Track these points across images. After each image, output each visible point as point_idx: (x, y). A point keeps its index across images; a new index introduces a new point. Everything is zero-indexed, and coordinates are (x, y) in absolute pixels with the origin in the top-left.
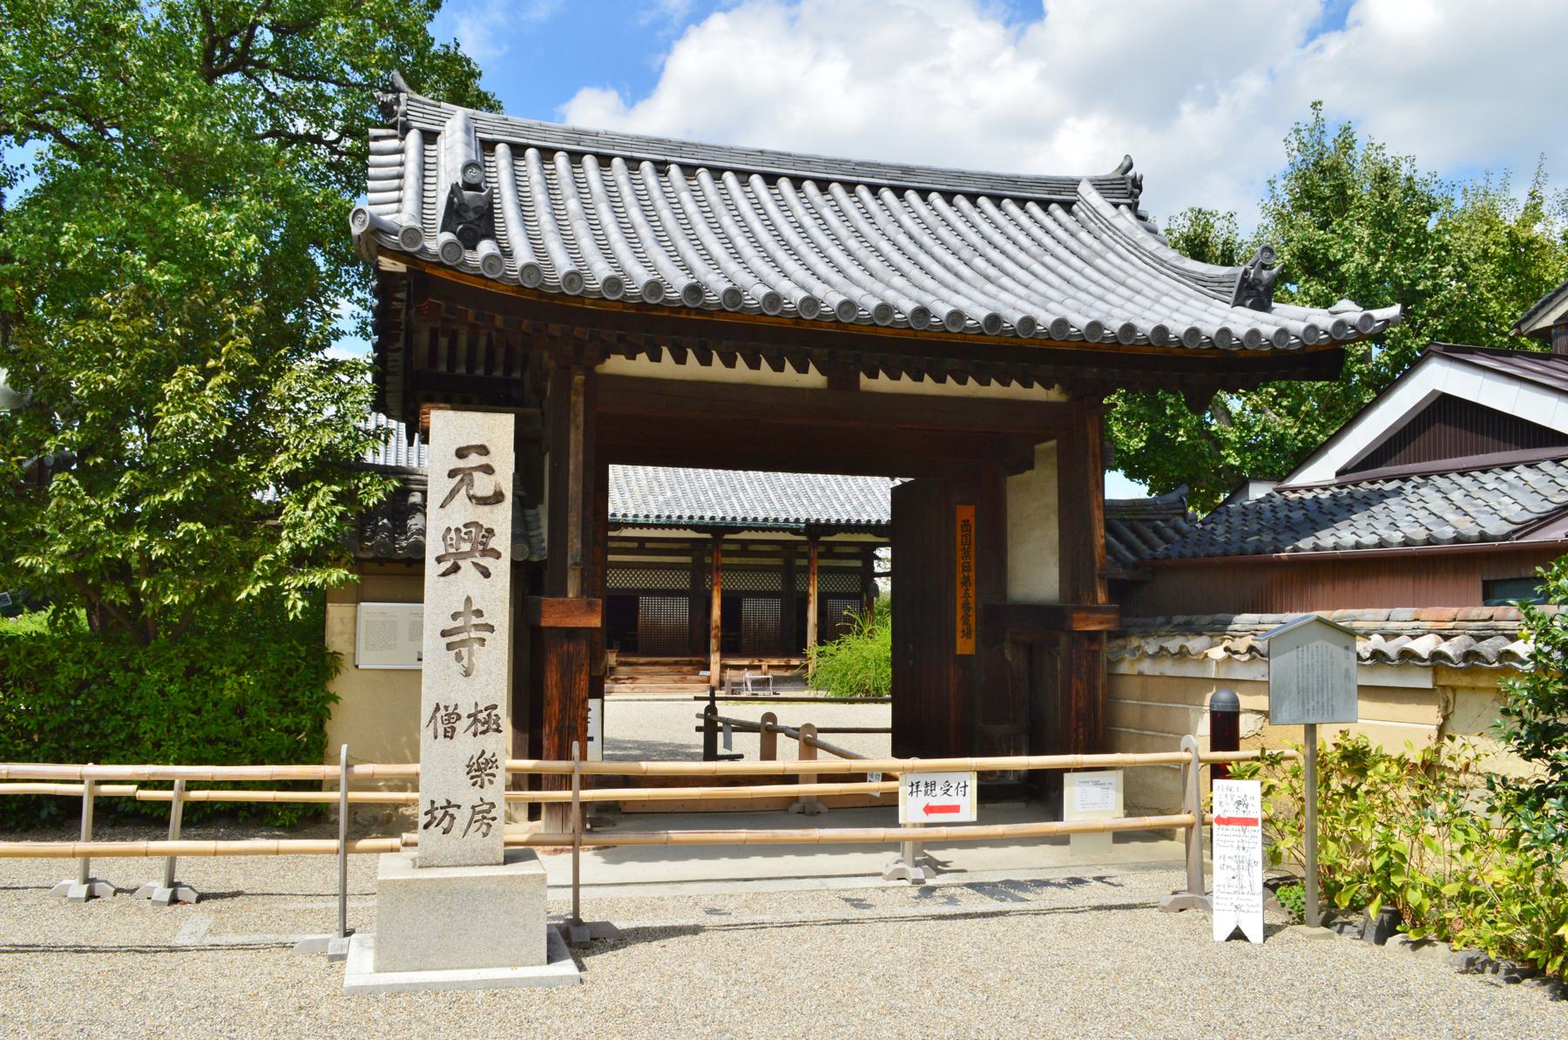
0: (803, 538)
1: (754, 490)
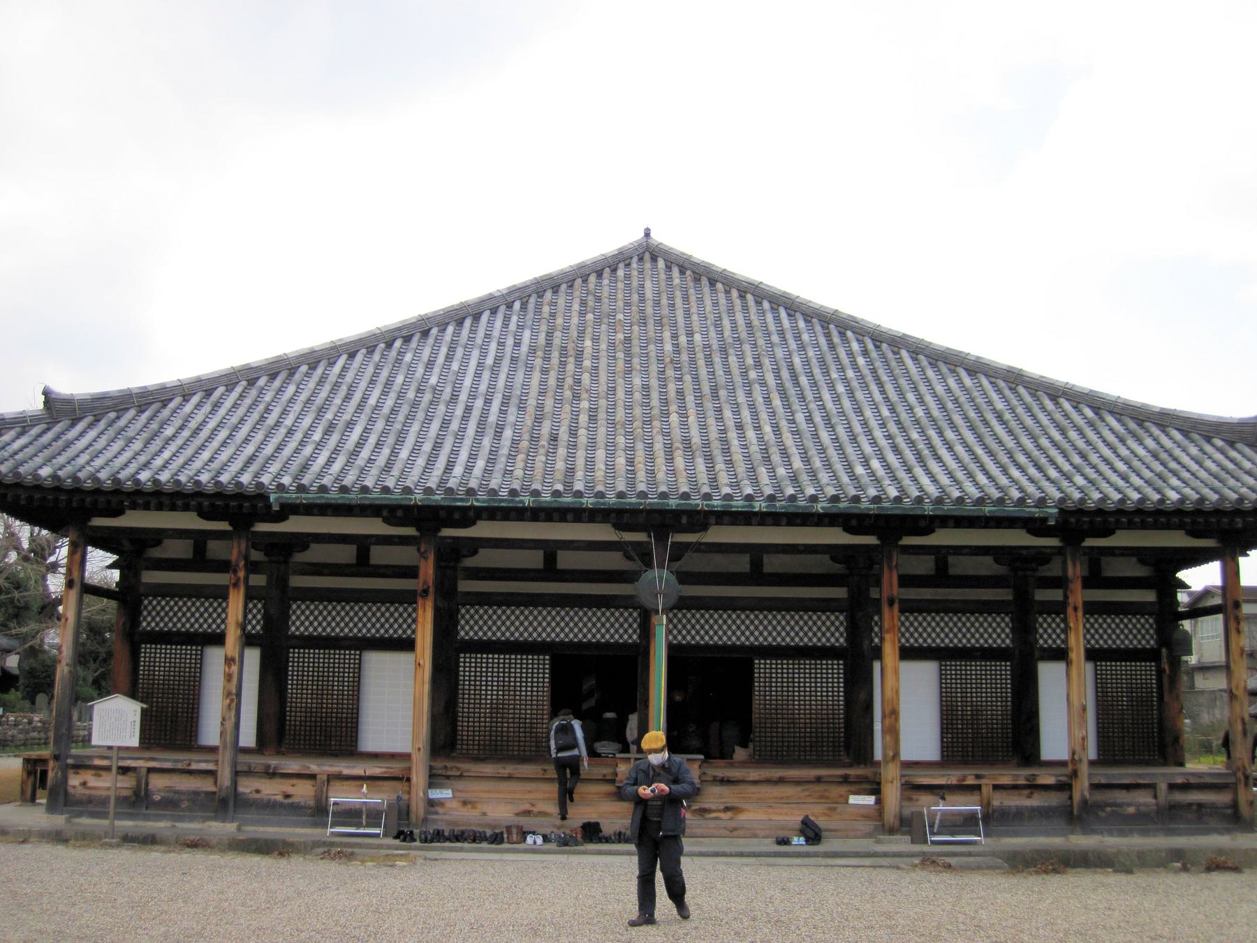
0: (1053, 542)
1: (957, 458)
